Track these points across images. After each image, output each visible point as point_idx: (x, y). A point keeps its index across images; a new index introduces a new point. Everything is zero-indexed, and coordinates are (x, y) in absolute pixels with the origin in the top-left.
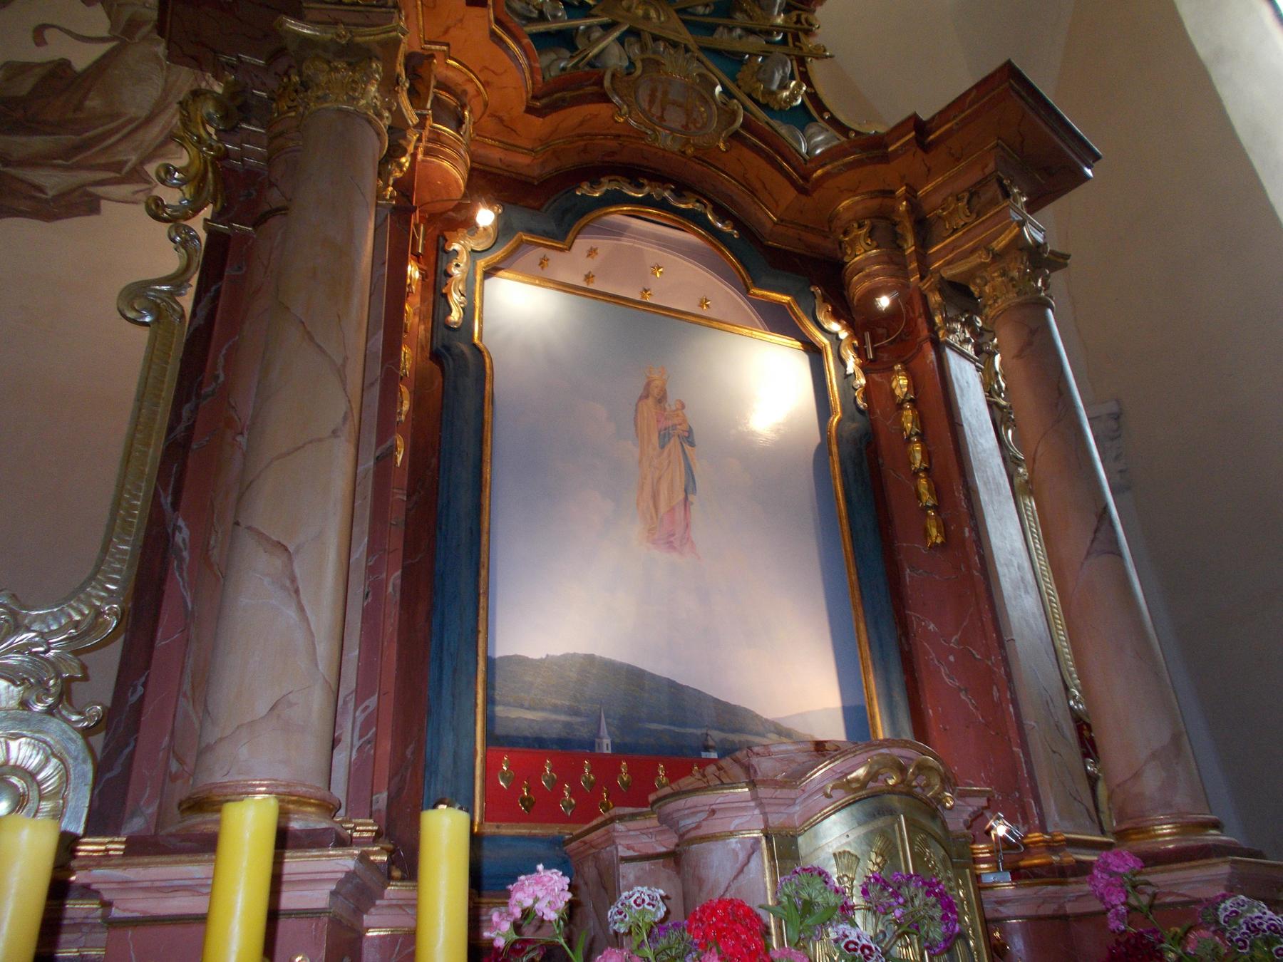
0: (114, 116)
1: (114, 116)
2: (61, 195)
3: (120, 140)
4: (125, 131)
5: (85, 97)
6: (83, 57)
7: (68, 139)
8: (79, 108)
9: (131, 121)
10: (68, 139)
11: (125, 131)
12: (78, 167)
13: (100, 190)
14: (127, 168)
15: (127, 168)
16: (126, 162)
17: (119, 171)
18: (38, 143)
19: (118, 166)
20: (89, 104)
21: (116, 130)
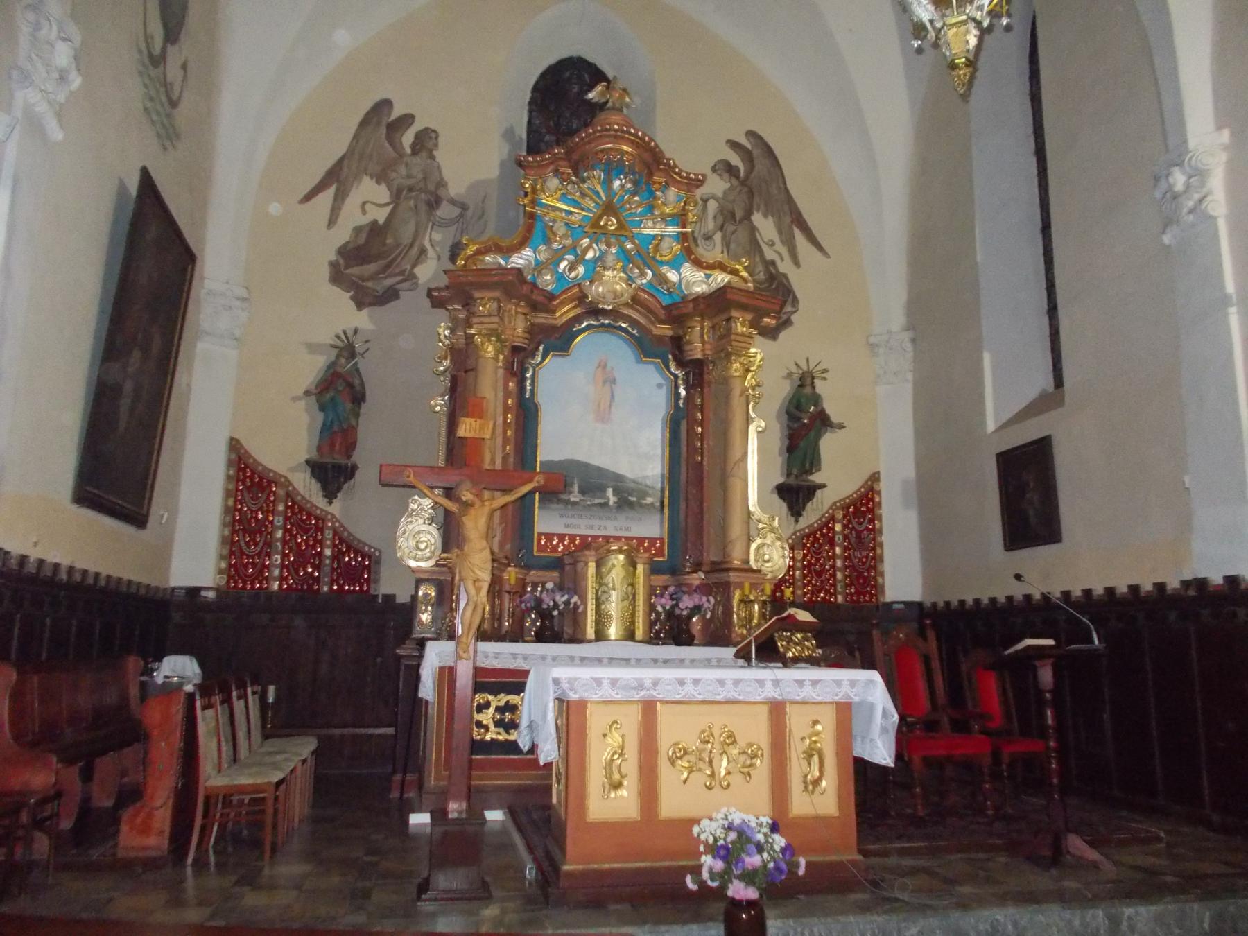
0: (398, 245)
1: (398, 245)
2: (385, 292)
3: (402, 258)
4: (402, 255)
5: (386, 238)
6: (381, 215)
7: (384, 262)
8: (384, 244)
9: (405, 246)
10: (384, 262)
11: (402, 255)
12: (390, 276)
13: (398, 287)
14: (407, 273)
15: (407, 273)
16: (405, 271)
17: (403, 275)
18: (371, 268)
19: (402, 273)
20: (388, 241)
21: (400, 254)
